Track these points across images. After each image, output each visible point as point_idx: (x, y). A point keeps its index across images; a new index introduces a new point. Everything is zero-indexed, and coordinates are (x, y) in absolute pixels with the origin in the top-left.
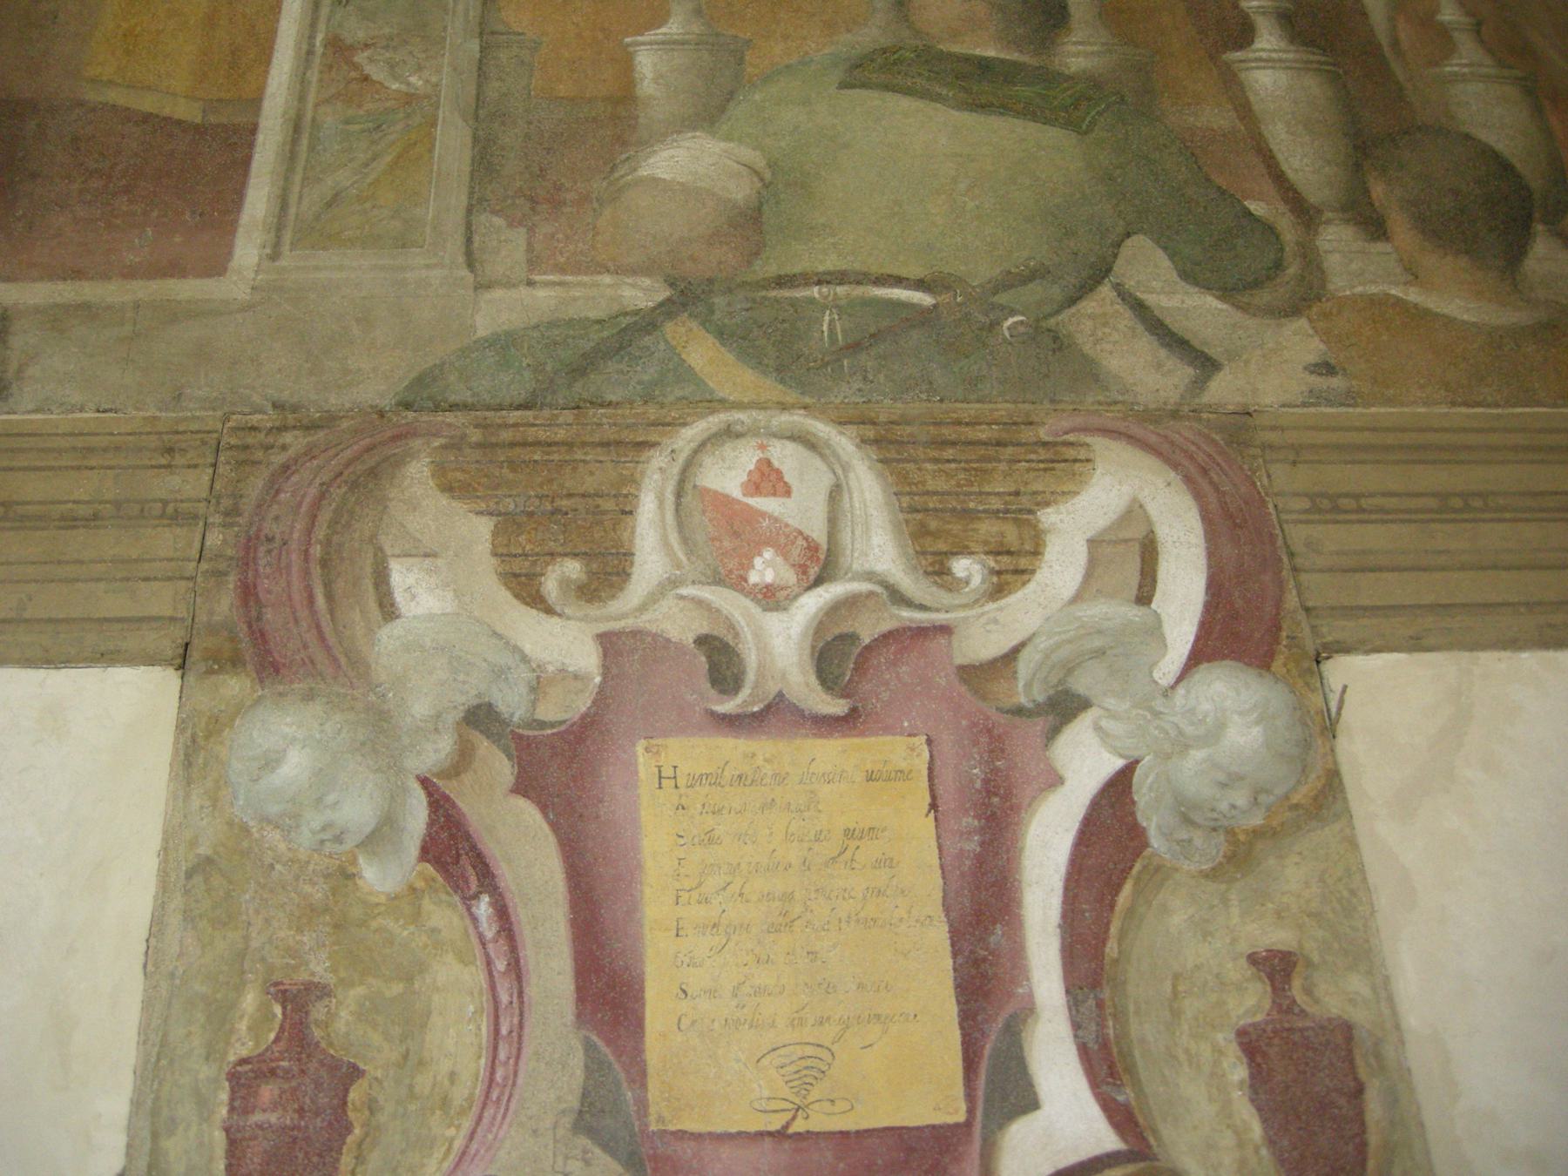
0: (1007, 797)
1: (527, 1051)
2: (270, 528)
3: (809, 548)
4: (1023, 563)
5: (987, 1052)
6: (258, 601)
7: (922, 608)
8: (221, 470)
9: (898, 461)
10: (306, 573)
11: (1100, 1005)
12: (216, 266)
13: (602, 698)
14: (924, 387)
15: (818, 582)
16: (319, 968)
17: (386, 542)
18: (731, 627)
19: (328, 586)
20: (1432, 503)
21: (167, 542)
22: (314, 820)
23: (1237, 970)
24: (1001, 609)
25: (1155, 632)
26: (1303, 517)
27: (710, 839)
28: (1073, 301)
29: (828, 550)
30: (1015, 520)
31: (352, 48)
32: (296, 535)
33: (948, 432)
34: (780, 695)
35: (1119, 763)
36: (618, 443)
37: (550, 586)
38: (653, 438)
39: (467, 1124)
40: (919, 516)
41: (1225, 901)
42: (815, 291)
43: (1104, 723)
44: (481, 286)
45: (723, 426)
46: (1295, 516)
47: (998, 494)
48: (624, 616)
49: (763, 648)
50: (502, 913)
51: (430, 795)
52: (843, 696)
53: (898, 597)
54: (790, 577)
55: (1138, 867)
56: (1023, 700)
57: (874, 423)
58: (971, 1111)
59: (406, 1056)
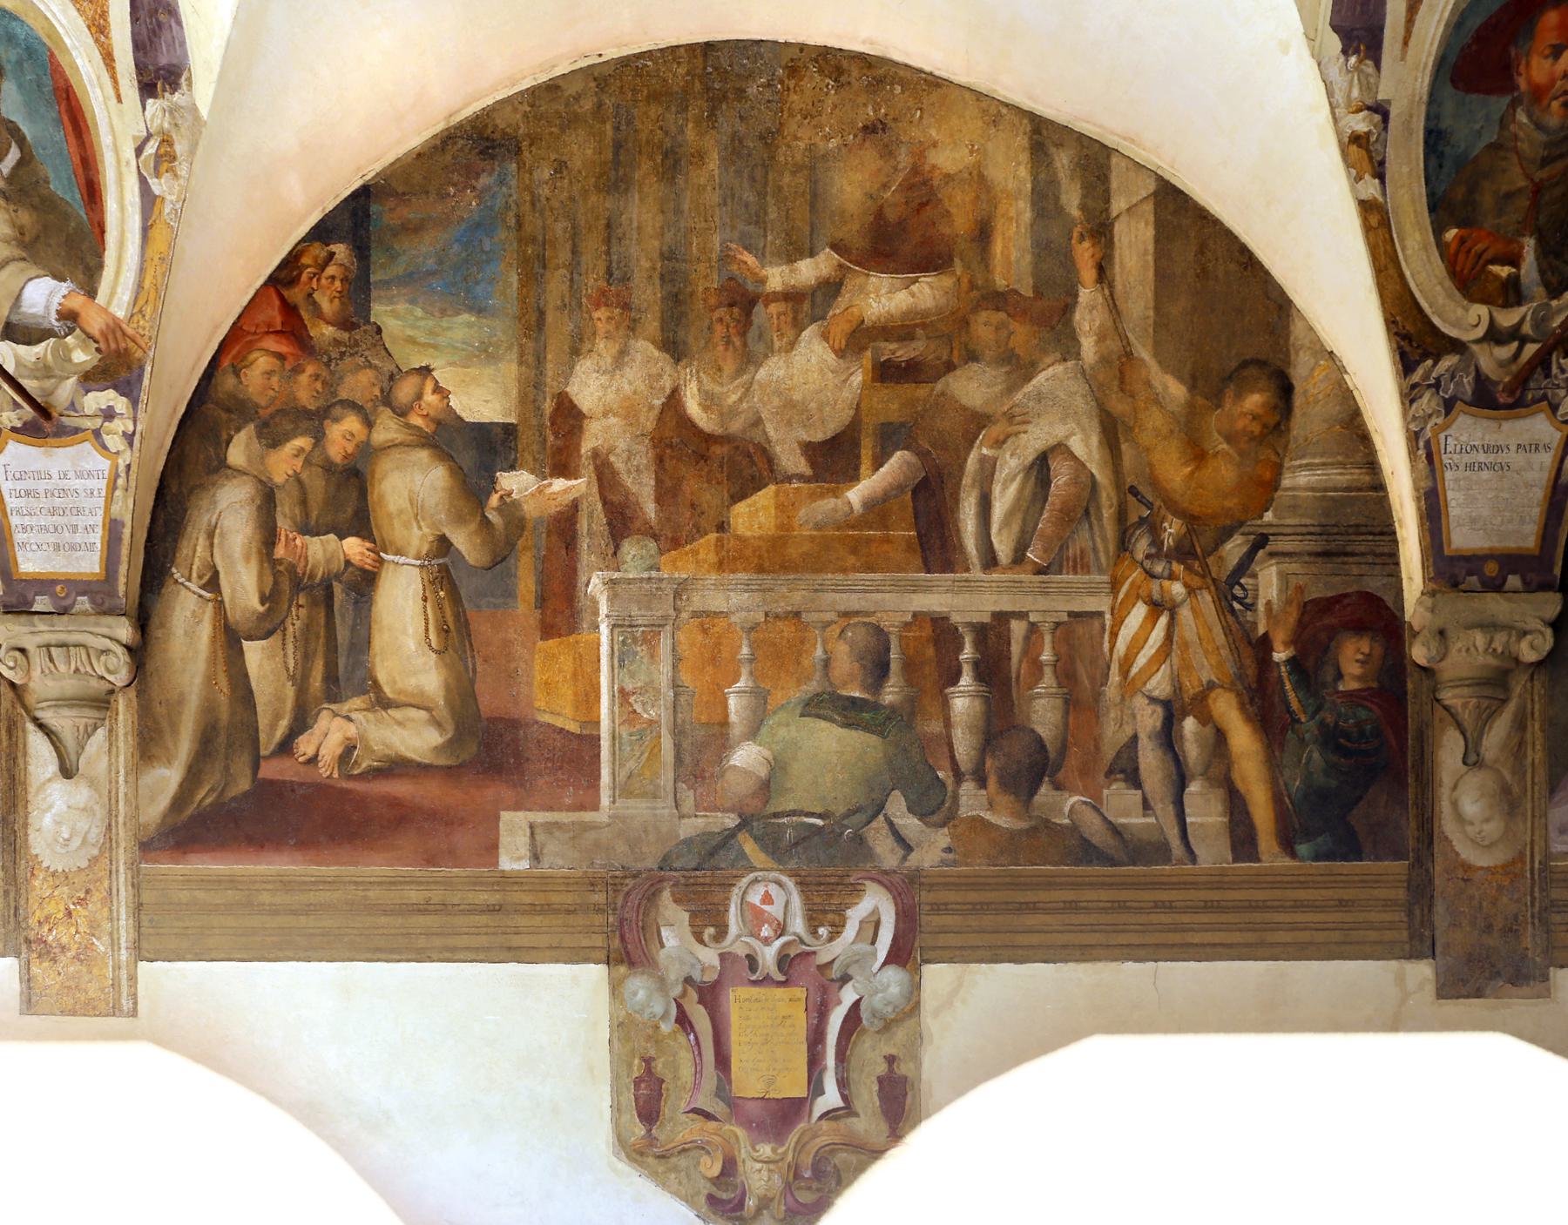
2: (626, 916)
12: (595, 807)
13: (720, 975)
16: (652, 1053)
17: (659, 920)
20: (970, 907)
21: (599, 919)
22: (648, 1011)
25: (874, 954)
27: (748, 1018)
28: (869, 822)
31: (628, 694)
33: (822, 880)
37: (706, 937)
42: (785, 820)
44: (682, 817)
49: (764, 959)
50: (696, 1038)
53: (802, 942)
54: (772, 934)
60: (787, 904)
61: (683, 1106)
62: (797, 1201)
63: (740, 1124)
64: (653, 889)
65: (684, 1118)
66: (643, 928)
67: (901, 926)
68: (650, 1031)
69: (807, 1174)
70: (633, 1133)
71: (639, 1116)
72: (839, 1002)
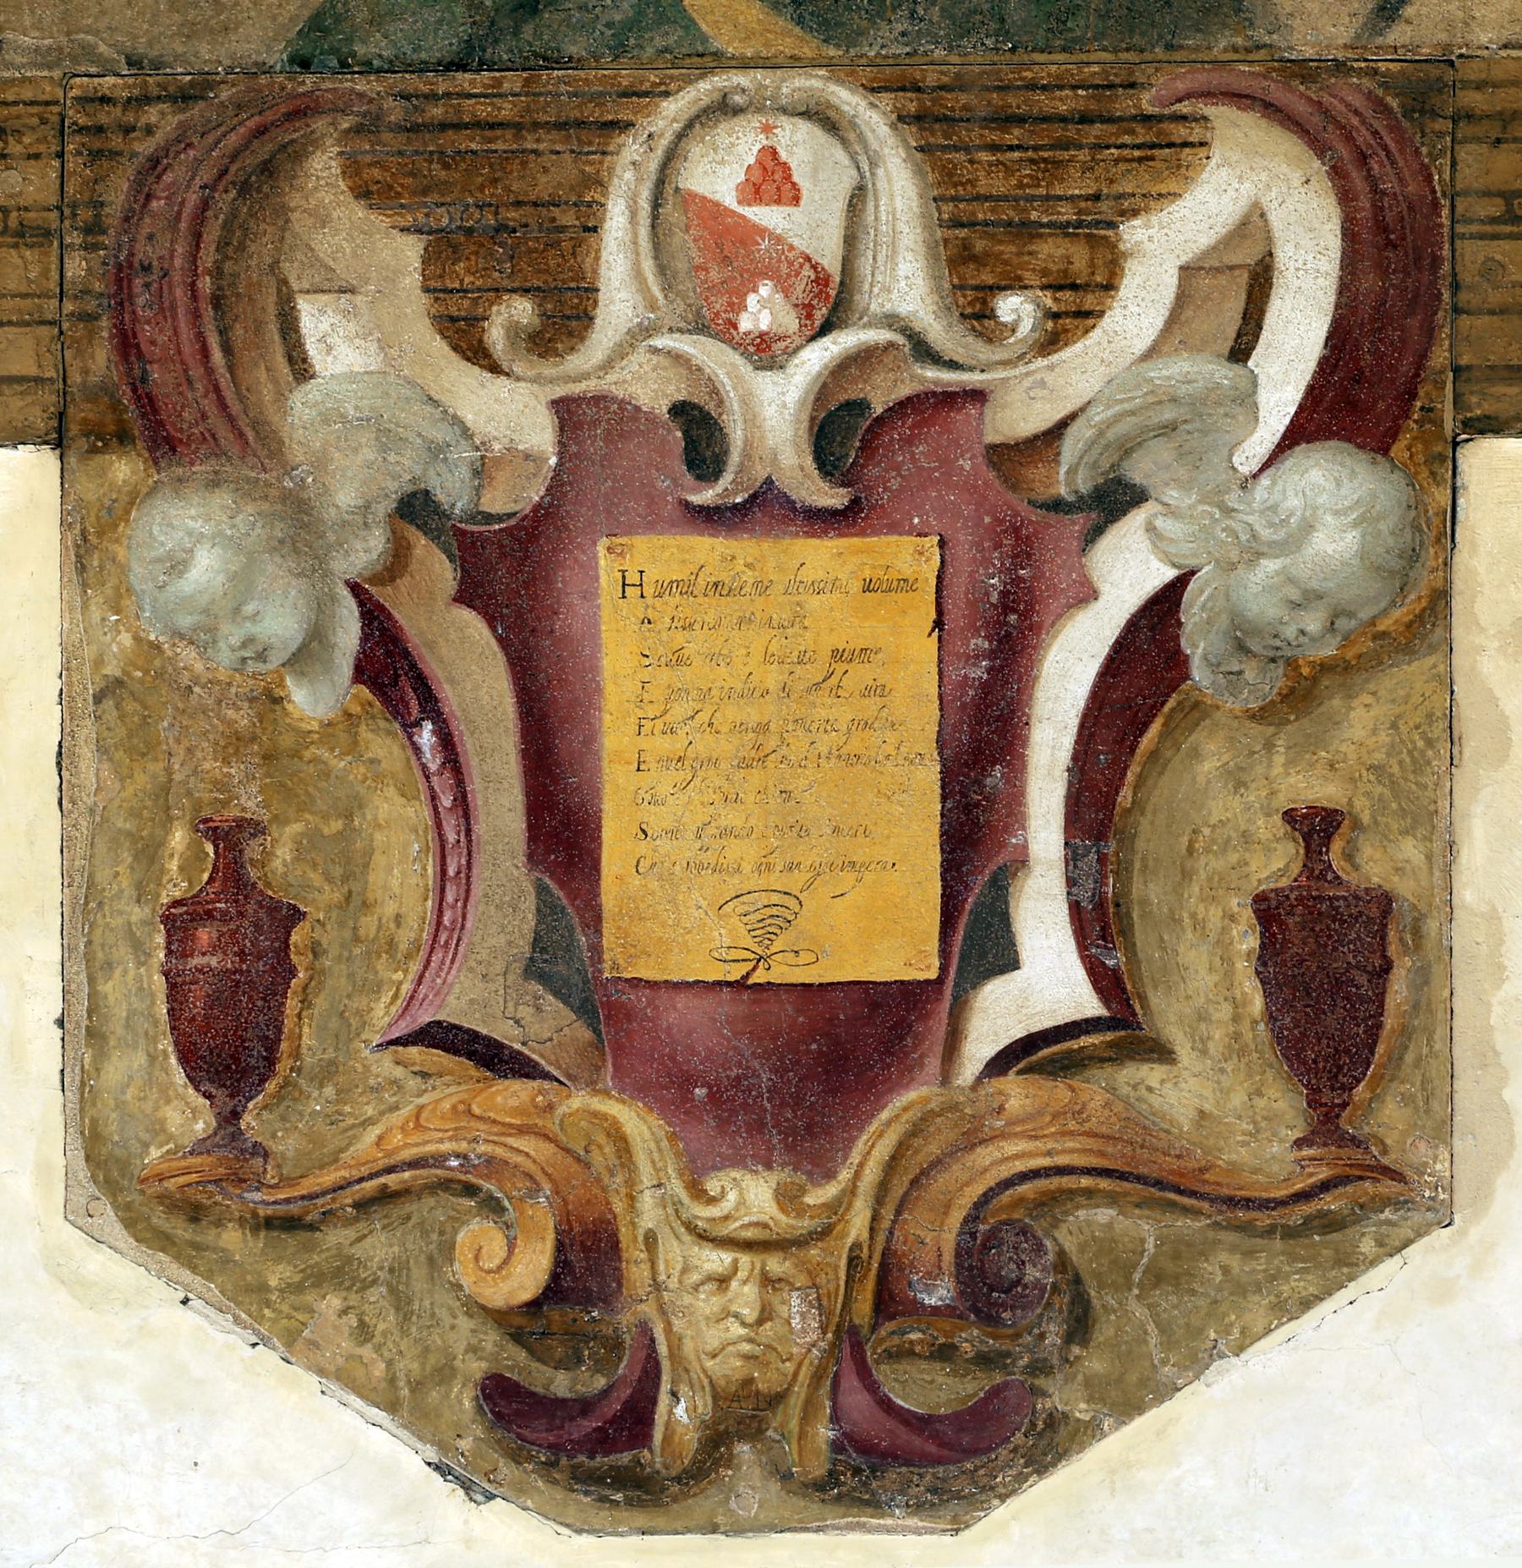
0: (1024, 615)
1: (478, 890)
2: (146, 252)
3: (817, 281)
4: (1089, 302)
5: (968, 907)
6: (140, 355)
7: (953, 365)
8: (70, 166)
9: (944, 148)
10: (196, 315)
11: (1102, 859)
13: (556, 486)
14: (994, 26)
15: (825, 329)
16: (250, 802)
17: (290, 270)
18: (715, 392)
19: (223, 332)
22: (232, 634)
23: (1269, 827)
24: (1051, 368)
25: (1246, 400)
26: (1488, 229)
27: (679, 659)
29: (842, 283)
30: (1089, 237)
32: (178, 262)
33: (1015, 102)
34: (769, 481)
35: (1170, 574)
36: (580, 124)
37: (496, 335)
38: (625, 115)
39: (415, 967)
40: (962, 233)
41: (1269, 746)
43: (1159, 523)
45: (717, 96)
46: (1474, 228)
47: (1072, 199)
48: (586, 376)
49: (752, 420)
50: (447, 742)
51: (361, 604)
52: (843, 485)
53: (924, 351)
54: (790, 322)
55: (1171, 703)
56: (1063, 491)
57: (918, 90)
58: (944, 969)
59: (349, 896)
60: (858, 199)
61: (383, 1015)
62: (887, 1405)
63: (639, 1090)
64: (263, 150)
65: (385, 1066)
66: (217, 302)
67: (1369, 282)
68: (242, 718)
69: (939, 1294)
70: (158, 1130)
71: (185, 1057)
72: (1087, 594)
